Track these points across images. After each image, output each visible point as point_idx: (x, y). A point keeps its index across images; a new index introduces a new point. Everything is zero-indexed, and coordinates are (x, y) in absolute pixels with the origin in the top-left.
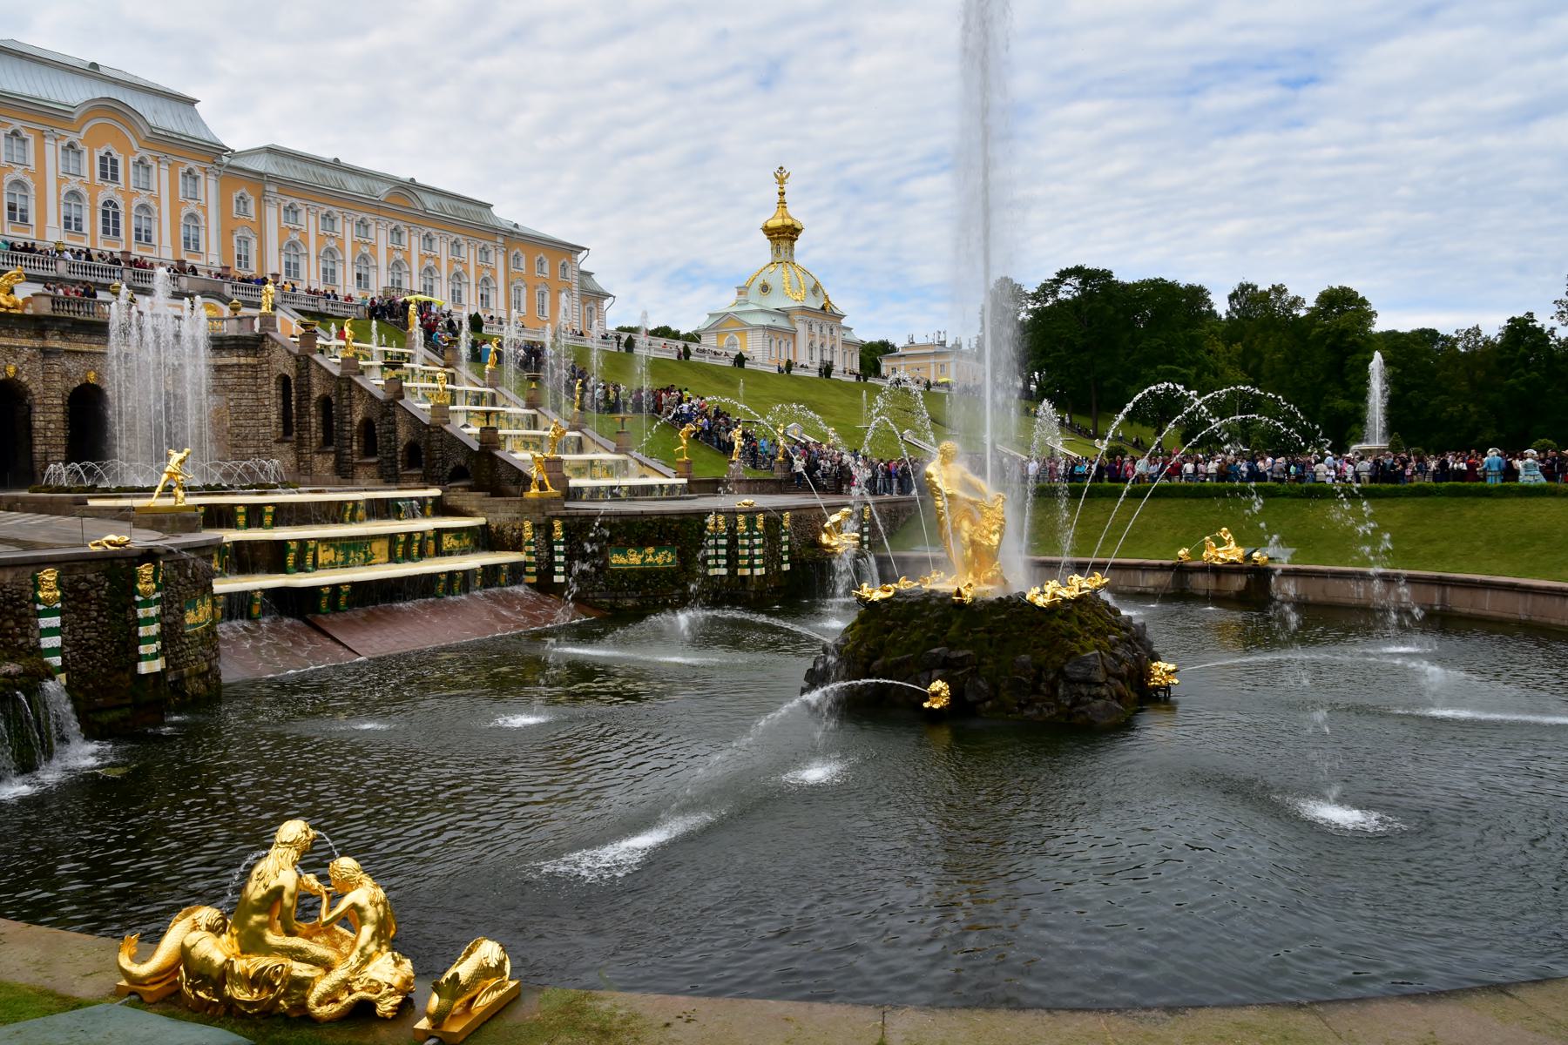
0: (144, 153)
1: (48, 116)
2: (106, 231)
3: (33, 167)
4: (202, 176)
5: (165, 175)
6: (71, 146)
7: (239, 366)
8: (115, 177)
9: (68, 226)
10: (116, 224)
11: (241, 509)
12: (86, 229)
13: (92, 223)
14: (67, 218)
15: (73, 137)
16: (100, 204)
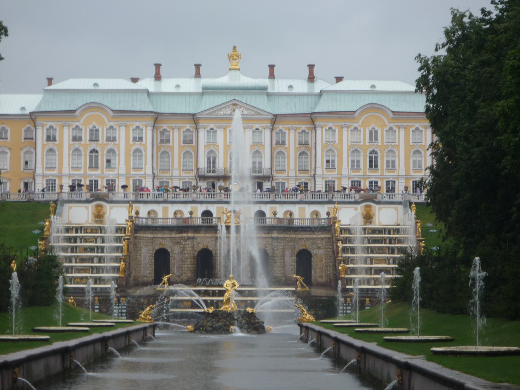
0: (391, 125)
1: (348, 115)
2: (371, 166)
3: (337, 142)
4: (424, 130)
5: (402, 132)
6: (356, 128)
7: (325, 238)
8: (376, 139)
9: (353, 166)
10: (376, 162)
11: (211, 292)
12: (362, 166)
13: (364, 162)
14: (353, 161)
15: (356, 125)
16: (368, 154)
